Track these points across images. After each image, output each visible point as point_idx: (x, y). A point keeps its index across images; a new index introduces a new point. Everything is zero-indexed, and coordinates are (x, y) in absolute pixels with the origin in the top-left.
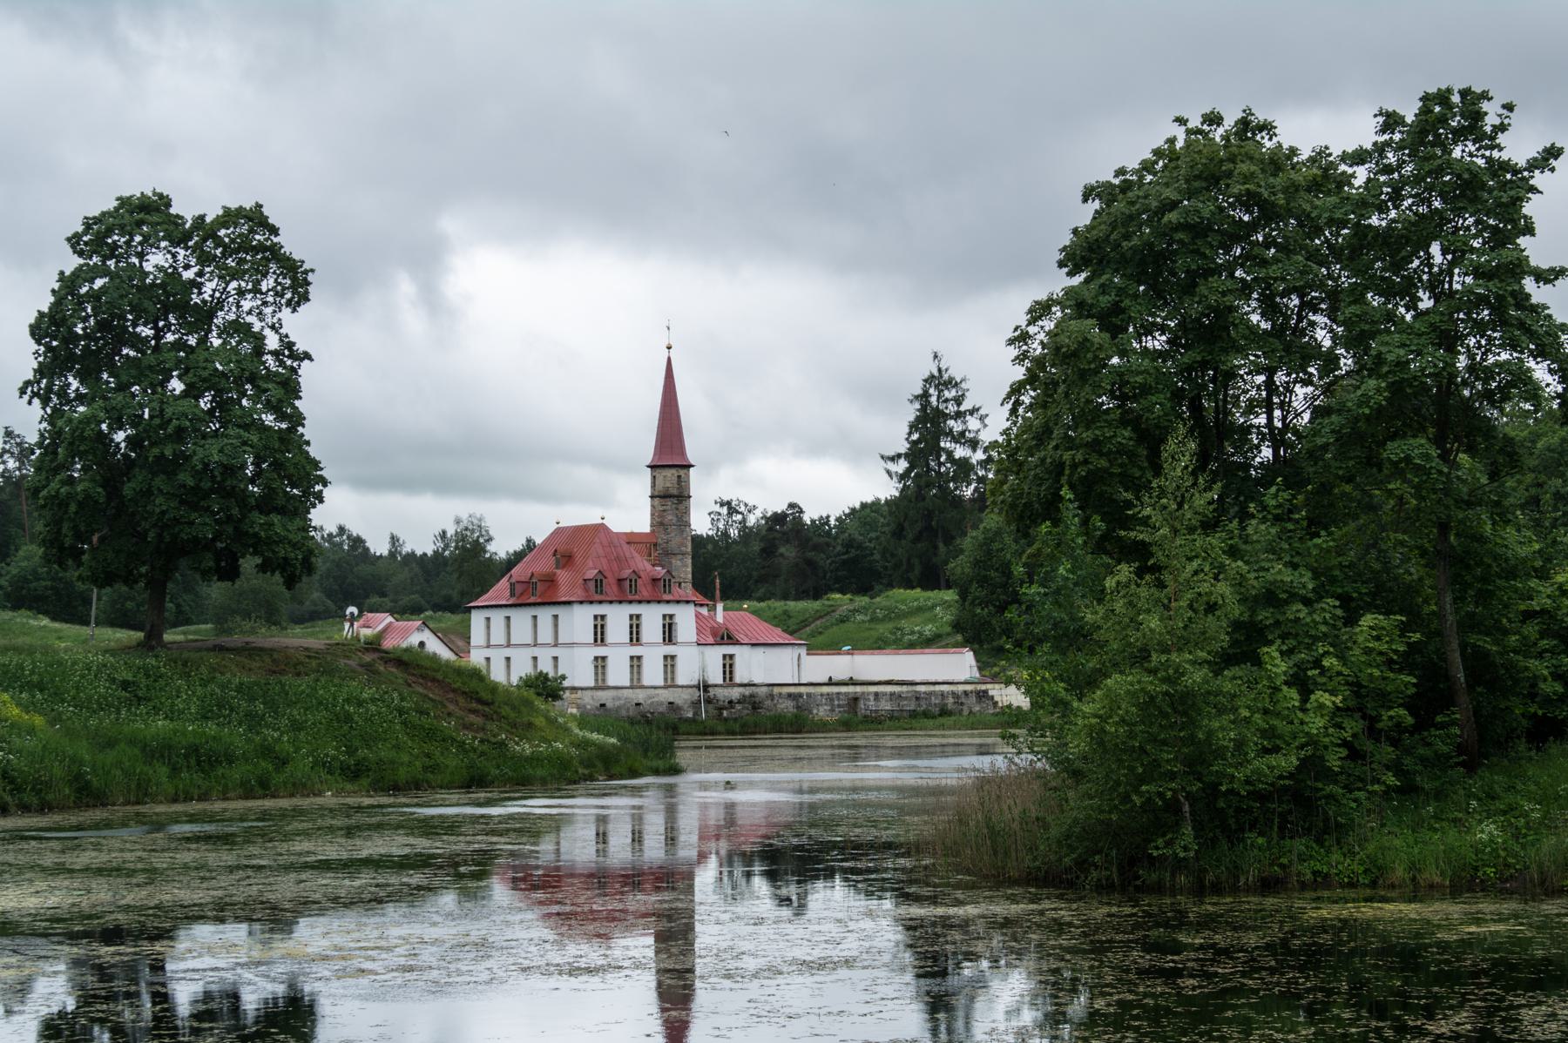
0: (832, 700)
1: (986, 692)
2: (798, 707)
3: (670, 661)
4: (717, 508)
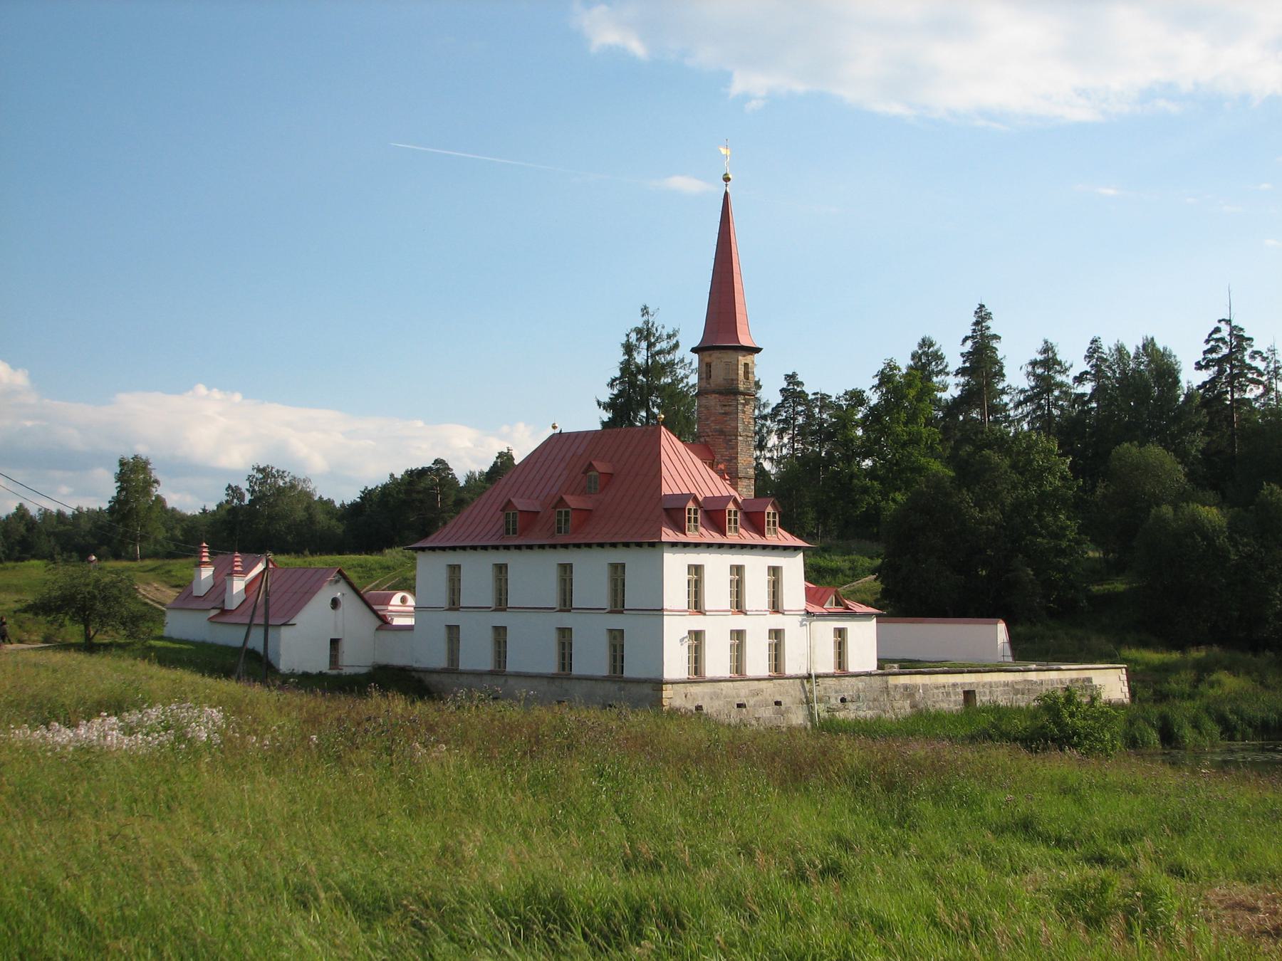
0: (948, 694)
1: (1089, 680)
3: (777, 634)
4: (254, 473)
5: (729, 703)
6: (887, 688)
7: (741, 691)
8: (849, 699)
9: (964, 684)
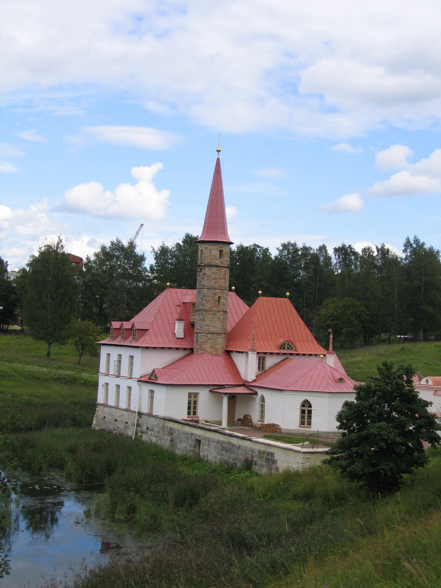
2: (172, 441)
5: (113, 418)
6: (164, 427)
7: (117, 414)
8: (149, 428)
9: (195, 435)
